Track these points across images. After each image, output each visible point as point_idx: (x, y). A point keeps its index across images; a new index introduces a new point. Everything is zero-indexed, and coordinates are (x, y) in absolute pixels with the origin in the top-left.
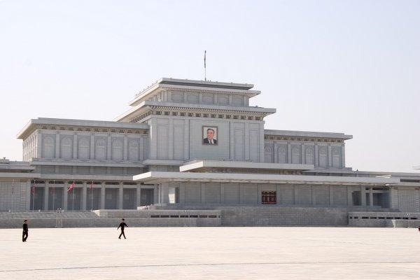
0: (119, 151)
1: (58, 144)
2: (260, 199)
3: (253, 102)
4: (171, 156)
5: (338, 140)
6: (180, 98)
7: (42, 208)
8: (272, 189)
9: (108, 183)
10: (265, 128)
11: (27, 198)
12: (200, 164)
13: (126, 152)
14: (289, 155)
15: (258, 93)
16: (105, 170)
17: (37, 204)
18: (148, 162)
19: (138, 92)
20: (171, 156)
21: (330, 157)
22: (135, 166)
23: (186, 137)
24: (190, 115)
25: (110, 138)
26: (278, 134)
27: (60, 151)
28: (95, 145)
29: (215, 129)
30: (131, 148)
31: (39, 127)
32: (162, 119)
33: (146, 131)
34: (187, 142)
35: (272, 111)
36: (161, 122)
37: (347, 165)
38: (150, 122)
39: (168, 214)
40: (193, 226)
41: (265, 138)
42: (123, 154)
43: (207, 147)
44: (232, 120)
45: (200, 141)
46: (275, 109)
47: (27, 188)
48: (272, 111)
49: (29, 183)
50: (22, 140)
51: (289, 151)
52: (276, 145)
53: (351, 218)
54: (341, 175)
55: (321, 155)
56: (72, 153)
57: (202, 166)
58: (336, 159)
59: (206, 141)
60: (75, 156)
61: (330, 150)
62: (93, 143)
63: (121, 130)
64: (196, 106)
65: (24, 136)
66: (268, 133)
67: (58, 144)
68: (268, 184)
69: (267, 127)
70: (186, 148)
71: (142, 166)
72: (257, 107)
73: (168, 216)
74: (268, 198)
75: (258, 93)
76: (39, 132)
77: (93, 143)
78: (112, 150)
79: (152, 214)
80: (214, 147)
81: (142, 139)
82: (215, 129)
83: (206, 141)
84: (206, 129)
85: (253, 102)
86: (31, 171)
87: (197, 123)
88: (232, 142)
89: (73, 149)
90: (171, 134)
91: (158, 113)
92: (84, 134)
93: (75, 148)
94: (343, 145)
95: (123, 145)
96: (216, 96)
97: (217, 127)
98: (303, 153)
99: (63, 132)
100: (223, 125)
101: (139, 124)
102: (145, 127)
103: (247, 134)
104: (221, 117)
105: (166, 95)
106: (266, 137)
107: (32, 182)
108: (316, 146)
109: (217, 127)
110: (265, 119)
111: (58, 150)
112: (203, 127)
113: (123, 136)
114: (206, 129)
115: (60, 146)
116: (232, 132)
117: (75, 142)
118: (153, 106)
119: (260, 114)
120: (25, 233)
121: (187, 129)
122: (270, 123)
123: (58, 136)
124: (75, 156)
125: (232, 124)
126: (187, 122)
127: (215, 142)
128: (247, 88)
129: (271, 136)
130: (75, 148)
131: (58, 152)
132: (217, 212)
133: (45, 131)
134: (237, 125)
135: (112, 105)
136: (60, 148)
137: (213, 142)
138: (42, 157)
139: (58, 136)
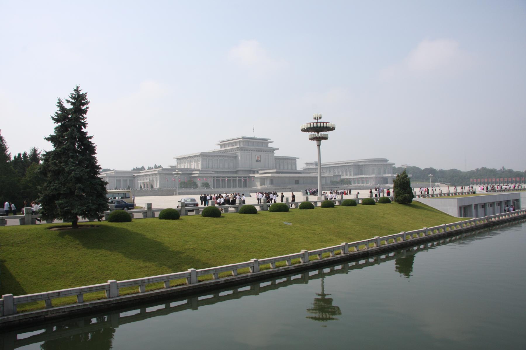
3: (270, 145)
5: (293, 160)
7: (236, 187)
8: (297, 179)
12: (275, 171)
19: (221, 140)
33: (236, 157)
35: (278, 149)
37: (297, 169)
47: (212, 179)
48: (278, 149)
49: (212, 179)
59: (257, 161)
69: (275, 155)
85: (270, 145)
87: (254, 153)
100: (262, 154)
106: (275, 158)
119: (272, 150)
122: (277, 154)
128: (267, 140)
129: (278, 159)
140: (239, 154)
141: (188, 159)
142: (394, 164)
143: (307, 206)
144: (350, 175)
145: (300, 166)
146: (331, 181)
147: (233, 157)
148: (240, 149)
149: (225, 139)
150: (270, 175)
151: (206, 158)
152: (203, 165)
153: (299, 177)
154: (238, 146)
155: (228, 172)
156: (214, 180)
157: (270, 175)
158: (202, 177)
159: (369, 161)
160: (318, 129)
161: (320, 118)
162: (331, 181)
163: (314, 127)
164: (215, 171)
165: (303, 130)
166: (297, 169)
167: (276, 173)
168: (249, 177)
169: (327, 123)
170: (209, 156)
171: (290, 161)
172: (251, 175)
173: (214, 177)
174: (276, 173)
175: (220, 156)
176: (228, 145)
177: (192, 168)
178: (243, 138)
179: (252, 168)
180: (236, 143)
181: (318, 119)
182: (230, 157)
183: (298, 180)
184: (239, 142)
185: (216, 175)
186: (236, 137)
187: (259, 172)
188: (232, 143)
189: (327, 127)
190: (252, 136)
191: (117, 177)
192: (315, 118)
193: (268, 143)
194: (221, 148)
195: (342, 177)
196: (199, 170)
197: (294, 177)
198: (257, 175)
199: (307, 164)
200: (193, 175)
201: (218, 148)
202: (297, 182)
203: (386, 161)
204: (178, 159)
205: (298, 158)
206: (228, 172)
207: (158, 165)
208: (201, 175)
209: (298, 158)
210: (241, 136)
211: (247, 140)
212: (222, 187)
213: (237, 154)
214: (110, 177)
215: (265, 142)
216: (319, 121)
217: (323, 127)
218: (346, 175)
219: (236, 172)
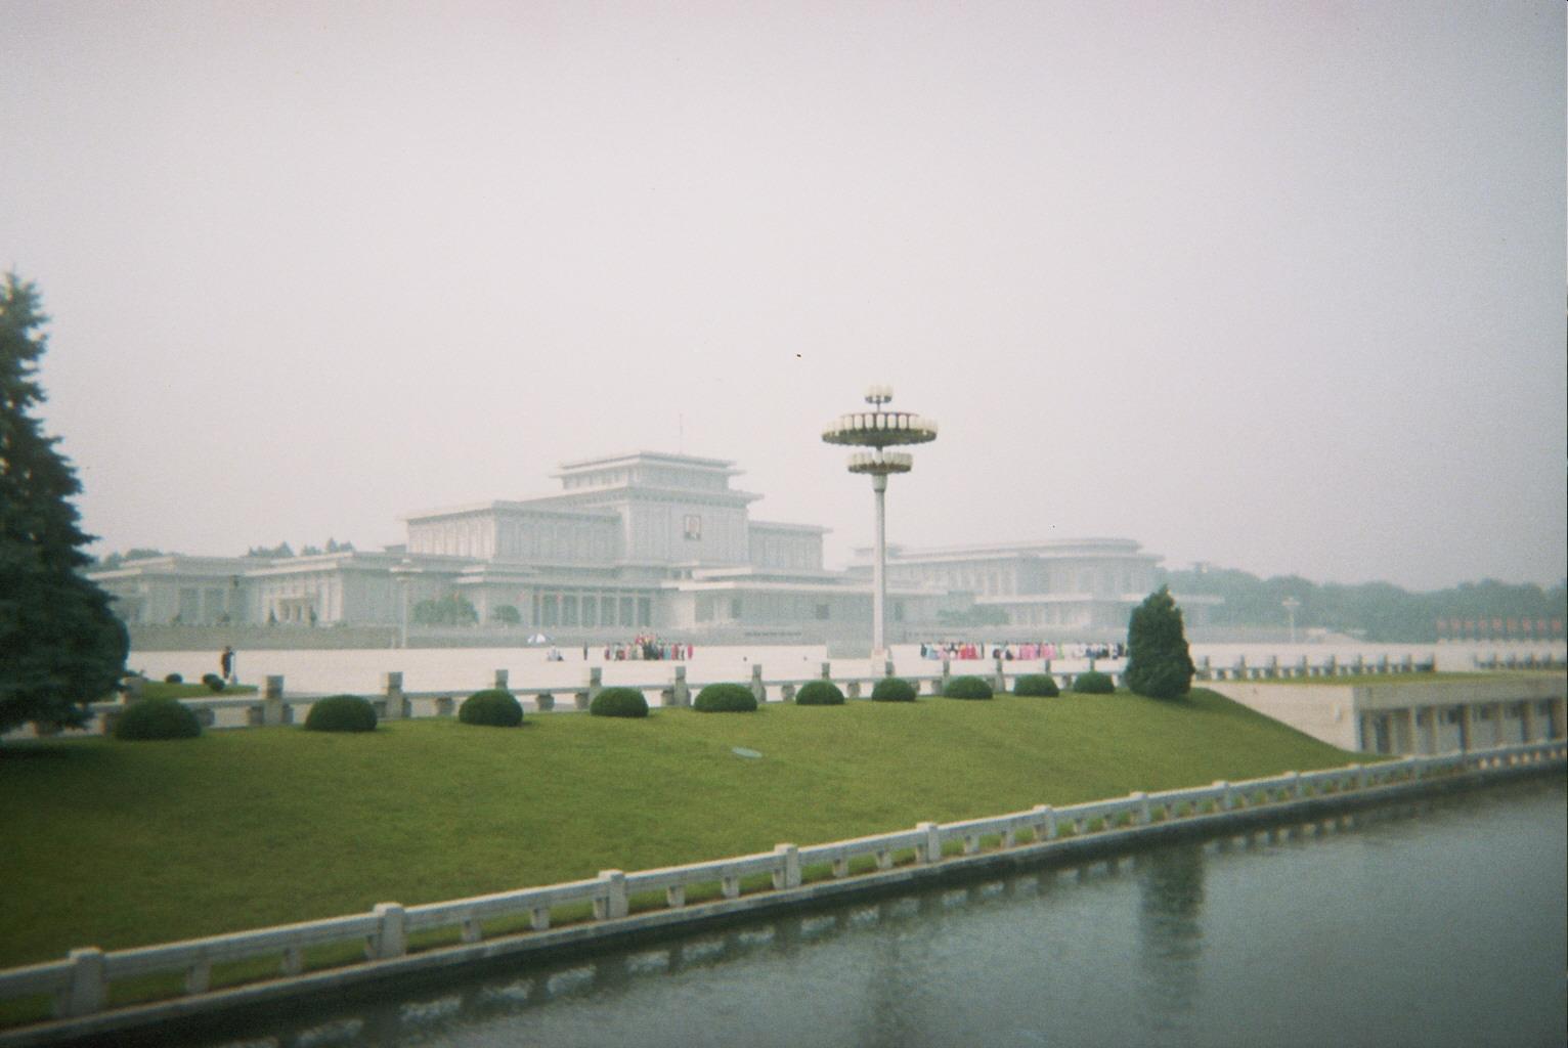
3: (734, 484)
5: (814, 535)
12: (747, 570)
18: (625, 562)
22: (605, 566)
33: (615, 520)
59: (688, 536)
82: (697, 520)
84: (688, 519)
85: (734, 484)
91: (638, 497)
94: (821, 541)
109: (700, 517)
114: (688, 519)
120: (586, 653)
122: (756, 513)
127: (699, 536)
128: (723, 465)
129: (759, 530)
140: (626, 512)
141: (449, 525)
142: (1161, 558)
143: (820, 694)
144: (1007, 592)
145: (836, 557)
146: (940, 613)
148: (634, 494)
150: (730, 585)
153: (830, 595)
155: (587, 572)
156: (536, 598)
157: (730, 585)
159: (1072, 548)
160: (877, 437)
161: (888, 399)
162: (940, 613)
163: (864, 430)
164: (540, 568)
165: (828, 438)
166: (826, 566)
167: (753, 577)
168: (660, 591)
169: (908, 415)
170: (522, 514)
172: (667, 584)
173: (537, 588)
174: (753, 577)
175: (560, 516)
176: (591, 476)
177: (462, 553)
178: (643, 456)
180: (617, 471)
181: (878, 402)
182: (597, 518)
184: (630, 469)
185: (546, 581)
187: (695, 574)
188: (602, 472)
189: (908, 430)
191: (181, 578)
192: (869, 400)
193: (724, 477)
194: (566, 486)
195: (979, 600)
196: (484, 562)
197: (813, 596)
198: (684, 586)
201: (556, 489)
202: (823, 612)
203: (1134, 547)
204: (412, 522)
205: (830, 531)
207: (339, 541)
209: (830, 531)
211: (655, 464)
212: (565, 623)
213: (619, 510)
214: (158, 578)
215: (715, 472)
216: (884, 407)
217: (897, 429)
218: (994, 592)
219: (615, 572)
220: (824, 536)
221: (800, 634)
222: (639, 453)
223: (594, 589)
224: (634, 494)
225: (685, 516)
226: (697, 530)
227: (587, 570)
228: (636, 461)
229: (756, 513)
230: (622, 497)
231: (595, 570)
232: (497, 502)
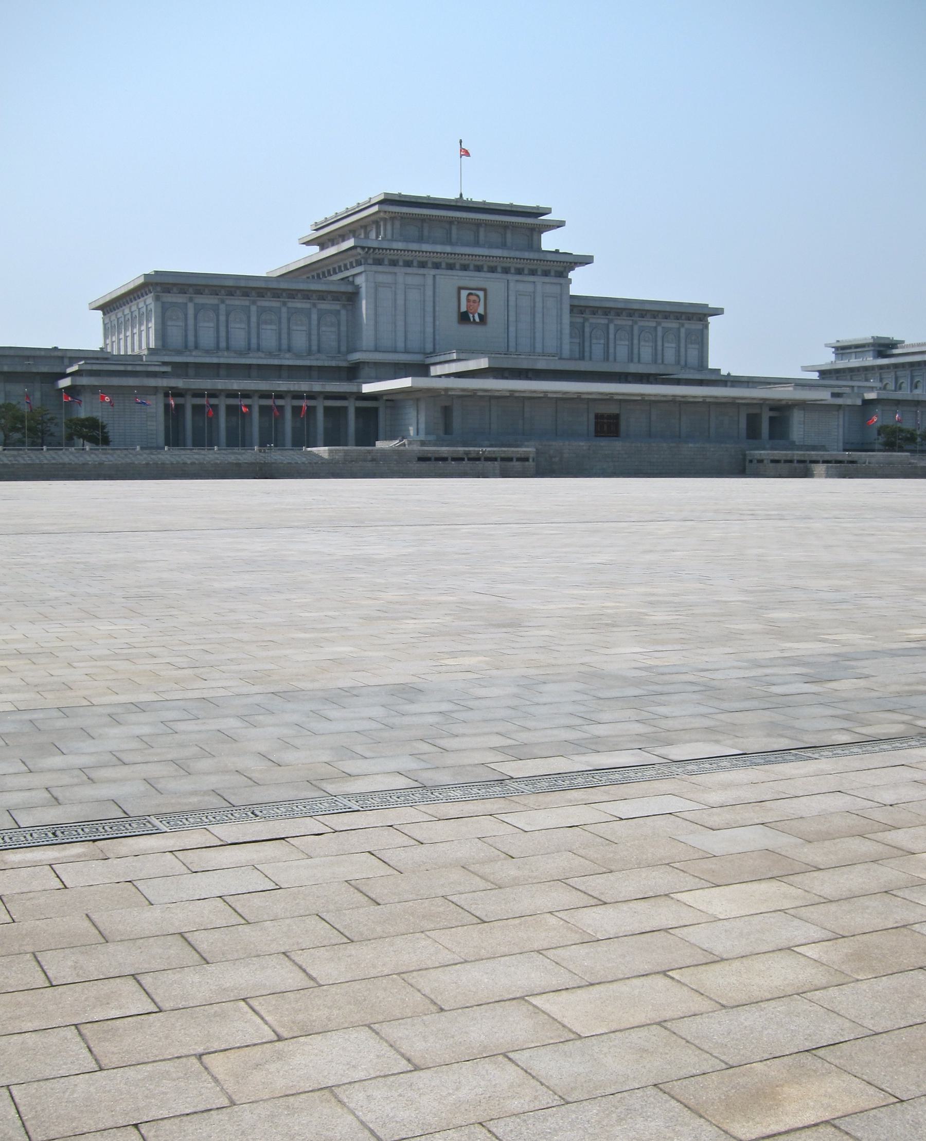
0: (302, 336)
1: (191, 321)
2: (592, 428)
3: (549, 241)
4: (401, 345)
5: (694, 318)
6: (415, 233)
8: (613, 409)
9: (265, 395)
10: (573, 292)
11: (157, 424)
12: (483, 363)
13: (314, 338)
14: (611, 345)
15: (560, 224)
16: (278, 371)
17: (174, 438)
18: (356, 357)
19: (320, 219)
20: (401, 345)
21: (683, 350)
22: (333, 363)
23: (429, 309)
24: (437, 266)
25: (284, 310)
26: (591, 304)
27: (196, 336)
28: (258, 324)
29: (481, 294)
30: (323, 329)
31: (164, 288)
32: (384, 275)
33: (352, 297)
34: (429, 319)
35: (586, 260)
36: (381, 278)
38: (360, 281)
39: (445, 455)
40: (495, 476)
41: (571, 311)
42: (310, 340)
43: (467, 329)
44: (512, 278)
45: (455, 317)
46: (592, 257)
47: (156, 405)
48: (586, 260)
49: (161, 397)
50: (100, 313)
51: (611, 336)
52: (587, 324)
53: (751, 461)
54: (700, 383)
55: (666, 345)
56: (218, 337)
57: (487, 366)
58: (693, 353)
59: (464, 318)
60: (223, 344)
61: (683, 335)
62: (254, 319)
63: (292, 294)
64: (448, 249)
65: (108, 307)
66: (576, 303)
67: (191, 321)
68: (609, 399)
69: (574, 290)
70: (429, 330)
71: (344, 364)
72: (557, 252)
73: (444, 459)
74: (606, 427)
75: (560, 224)
76: (157, 298)
77: (254, 319)
78: (289, 334)
79: (420, 455)
80: (480, 329)
81: (343, 312)
82: (481, 294)
83: (464, 318)
84: (464, 293)
85: (549, 241)
86: (164, 374)
87: (448, 282)
88: (512, 318)
89: (218, 331)
90: (400, 302)
91: (378, 262)
92: (237, 303)
93: (223, 334)
94: (706, 326)
95: (310, 324)
96: (482, 230)
97: (485, 290)
98: (636, 341)
99: (200, 300)
100: (495, 285)
101: (332, 282)
102: (350, 289)
103: (539, 305)
104: (493, 270)
105: (389, 227)
106: (573, 307)
107: (166, 395)
108: (659, 329)
110: (571, 275)
111: (191, 338)
112: (460, 289)
113: (308, 306)
114: (464, 293)
115: (195, 325)
116: (512, 299)
117: (222, 318)
118: (369, 248)
121: (429, 293)
122: (582, 283)
123: (191, 306)
124: (223, 344)
125: (512, 285)
126: (430, 281)
127: (483, 318)
130: (223, 334)
131: (191, 338)
132: (528, 449)
133: (169, 298)
134: (522, 286)
135: (271, 247)
136: (196, 330)
137: (477, 319)
138: (163, 346)
139: (191, 306)
147: (336, 296)
149: (330, 214)
151: (180, 299)
152: (162, 334)
154: (350, 243)
155: (307, 372)
158: (94, 389)
171: (672, 324)
173: (177, 393)
178: (389, 201)
179: (431, 353)
182: (323, 296)
183: (616, 417)
185: (179, 383)
186: (362, 198)
190: (449, 193)
199: (842, 350)
200: (65, 383)
205: (718, 312)
206: (307, 372)
208: (84, 381)
209: (718, 312)
210: (377, 194)
215: (527, 223)
220: (710, 319)
221: (527, 459)
222: (382, 197)
223: (280, 395)
224: (371, 257)
225: (460, 289)
226: (481, 310)
227: (310, 368)
228: (376, 208)
229: (582, 283)
230: (359, 264)
231: (320, 369)
232: (146, 276)
